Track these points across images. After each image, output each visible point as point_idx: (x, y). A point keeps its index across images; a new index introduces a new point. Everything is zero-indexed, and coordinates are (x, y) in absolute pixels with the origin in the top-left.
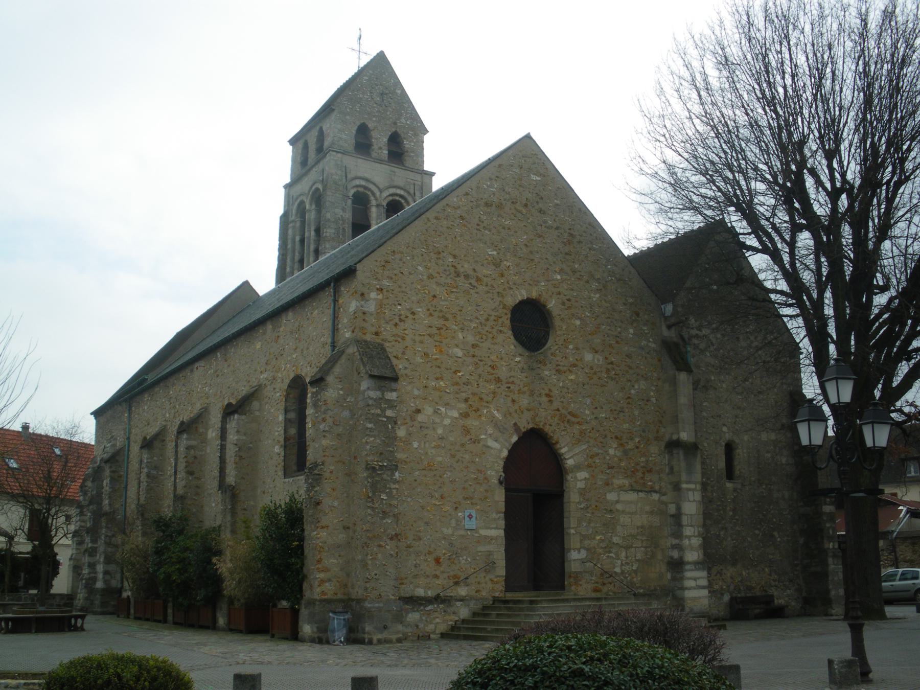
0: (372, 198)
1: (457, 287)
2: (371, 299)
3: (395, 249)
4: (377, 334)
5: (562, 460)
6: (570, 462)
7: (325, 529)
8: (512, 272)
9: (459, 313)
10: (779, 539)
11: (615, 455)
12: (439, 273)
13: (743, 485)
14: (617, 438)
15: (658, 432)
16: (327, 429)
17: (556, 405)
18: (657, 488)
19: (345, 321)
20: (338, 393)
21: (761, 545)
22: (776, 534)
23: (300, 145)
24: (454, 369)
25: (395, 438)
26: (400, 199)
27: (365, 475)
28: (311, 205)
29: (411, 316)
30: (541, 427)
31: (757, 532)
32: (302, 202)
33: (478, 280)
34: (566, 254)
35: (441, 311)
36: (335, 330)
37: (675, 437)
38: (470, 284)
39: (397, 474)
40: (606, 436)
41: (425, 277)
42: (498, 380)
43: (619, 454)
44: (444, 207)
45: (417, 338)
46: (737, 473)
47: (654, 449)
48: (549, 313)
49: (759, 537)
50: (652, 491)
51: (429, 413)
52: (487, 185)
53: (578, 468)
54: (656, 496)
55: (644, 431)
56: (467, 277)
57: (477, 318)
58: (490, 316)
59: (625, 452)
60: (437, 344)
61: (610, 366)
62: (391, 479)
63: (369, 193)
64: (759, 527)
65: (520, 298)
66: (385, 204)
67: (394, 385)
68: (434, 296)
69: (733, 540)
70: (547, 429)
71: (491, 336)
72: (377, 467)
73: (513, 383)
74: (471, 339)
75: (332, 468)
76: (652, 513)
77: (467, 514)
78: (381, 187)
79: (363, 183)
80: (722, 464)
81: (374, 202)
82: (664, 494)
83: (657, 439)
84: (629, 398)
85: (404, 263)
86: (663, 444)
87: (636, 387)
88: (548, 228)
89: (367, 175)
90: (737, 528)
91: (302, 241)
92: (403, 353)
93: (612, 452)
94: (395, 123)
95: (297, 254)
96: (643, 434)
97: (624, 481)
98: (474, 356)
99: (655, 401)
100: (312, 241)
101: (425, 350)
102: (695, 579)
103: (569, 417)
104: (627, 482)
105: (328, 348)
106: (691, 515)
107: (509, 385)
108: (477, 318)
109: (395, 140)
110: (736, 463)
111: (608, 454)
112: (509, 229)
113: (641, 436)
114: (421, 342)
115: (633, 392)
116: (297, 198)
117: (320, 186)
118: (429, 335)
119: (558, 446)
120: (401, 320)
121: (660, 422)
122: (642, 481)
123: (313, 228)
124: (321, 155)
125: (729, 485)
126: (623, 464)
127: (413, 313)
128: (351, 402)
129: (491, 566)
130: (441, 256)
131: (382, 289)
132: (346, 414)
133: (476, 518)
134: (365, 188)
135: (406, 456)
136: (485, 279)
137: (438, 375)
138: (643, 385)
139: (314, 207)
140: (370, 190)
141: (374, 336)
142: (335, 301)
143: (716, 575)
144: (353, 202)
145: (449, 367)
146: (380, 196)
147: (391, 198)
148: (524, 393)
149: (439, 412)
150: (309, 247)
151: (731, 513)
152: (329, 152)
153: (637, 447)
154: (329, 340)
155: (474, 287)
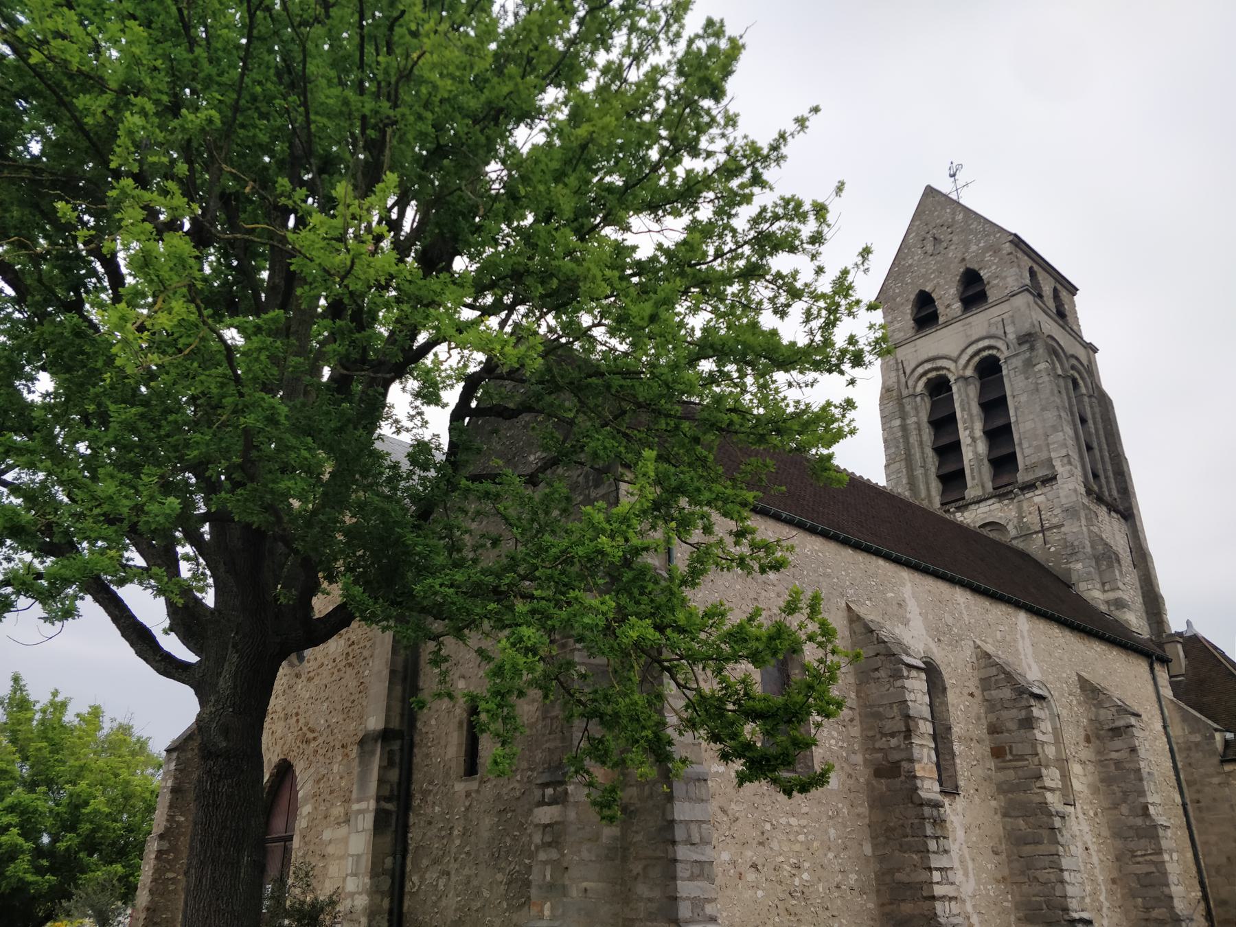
26: (991, 352)
31: (499, 877)
53: (306, 801)
66: (969, 372)
69: (458, 896)
79: (928, 366)
89: (932, 354)
94: (964, 259)
125: (460, 787)
146: (957, 367)
147: (977, 359)
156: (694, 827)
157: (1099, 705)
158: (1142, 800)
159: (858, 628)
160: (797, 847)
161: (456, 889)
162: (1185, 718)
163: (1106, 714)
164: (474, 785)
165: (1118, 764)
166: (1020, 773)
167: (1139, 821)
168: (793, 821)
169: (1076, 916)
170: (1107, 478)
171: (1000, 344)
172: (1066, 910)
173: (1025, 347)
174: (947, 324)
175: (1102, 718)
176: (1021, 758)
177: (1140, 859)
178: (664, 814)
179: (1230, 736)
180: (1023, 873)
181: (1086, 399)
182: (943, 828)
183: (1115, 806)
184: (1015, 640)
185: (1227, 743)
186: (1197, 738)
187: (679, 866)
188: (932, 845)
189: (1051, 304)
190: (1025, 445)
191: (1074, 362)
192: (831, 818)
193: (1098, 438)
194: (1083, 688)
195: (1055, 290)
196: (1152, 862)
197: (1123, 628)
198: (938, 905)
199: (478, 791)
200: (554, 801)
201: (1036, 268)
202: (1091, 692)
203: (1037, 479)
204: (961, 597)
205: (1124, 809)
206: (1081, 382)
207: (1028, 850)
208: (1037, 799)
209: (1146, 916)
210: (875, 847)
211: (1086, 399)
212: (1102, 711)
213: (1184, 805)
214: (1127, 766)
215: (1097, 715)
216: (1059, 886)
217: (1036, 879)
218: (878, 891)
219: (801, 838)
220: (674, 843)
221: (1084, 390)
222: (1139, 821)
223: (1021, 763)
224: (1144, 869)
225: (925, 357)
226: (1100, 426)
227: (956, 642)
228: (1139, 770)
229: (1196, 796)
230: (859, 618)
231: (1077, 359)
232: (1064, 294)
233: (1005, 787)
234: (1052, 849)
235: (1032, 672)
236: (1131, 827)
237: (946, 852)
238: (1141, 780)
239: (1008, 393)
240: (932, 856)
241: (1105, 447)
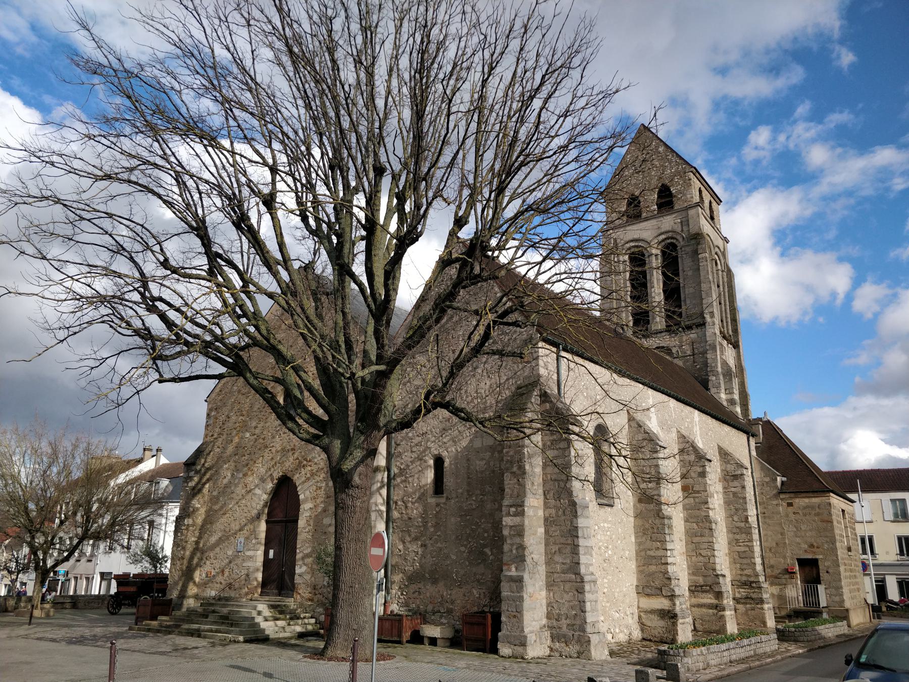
6: (302, 497)
10: (491, 557)
13: (447, 498)
21: (467, 563)
22: (487, 551)
31: (463, 549)
49: (465, 554)
53: (306, 500)
64: (465, 543)
69: (432, 558)
79: (633, 244)
89: (636, 237)
90: (439, 545)
125: (432, 501)
140: (641, 246)
143: (414, 593)
151: (432, 530)
156: (585, 529)
157: (728, 462)
158: (745, 513)
159: (634, 424)
160: (607, 538)
161: (431, 554)
162: (763, 468)
163: (730, 468)
164: (443, 500)
165: (734, 494)
166: (697, 500)
167: (742, 525)
168: (606, 525)
169: (719, 573)
170: (727, 322)
171: (678, 237)
172: (714, 570)
173: (693, 242)
174: (647, 219)
175: (728, 469)
176: (698, 492)
177: (741, 544)
178: (572, 523)
179: (784, 479)
180: (693, 550)
181: (720, 273)
182: (672, 529)
183: (731, 516)
184: (693, 427)
185: (783, 483)
186: (767, 479)
187: (581, 549)
188: (668, 538)
189: (708, 211)
190: (688, 302)
191: (717, 250)
192: (619, 523)
193: (725, 297)
194: (720, 453)
195: (710, 202)
196: (747, 546)
197: (734, 415)
198: (669, 567)
199: (445, 504)
200: (515, 515)
201: (703, 189)
202: (724, 454)
203: (694, 324)
204: (673, 403)
205: (736, 518)
206: (718, 262)
207: (696, 540)
208: (704, 514)
209: (741, 573)
210: (636, 537)
211: (720, 273)
212: (729, 466)
213: (757, 515)
214: (740, 495)
215: (726, 467)
216: (712, 558)
217: (700, 554)
218: (637, 560)
219: (608, 533)
220: (578, 537)
221: (719, 267)
222: (742, 525)
223: (697, 495)
224: (743, 549)
225: (630, 238)
226: (726, 290)
227: (669, 430)
228: (745, 498)
229: (763, 511)
230: (634, 419)
231: (719, 248)
232: (714, 204)
233: (688, 507)
234: (710, 540)
235: (653, 424)
236: (738, 527)
237: (673, 541)
238: (746, 503)
239: (680, 268)
240: (668, 543)
241: (728, 303)
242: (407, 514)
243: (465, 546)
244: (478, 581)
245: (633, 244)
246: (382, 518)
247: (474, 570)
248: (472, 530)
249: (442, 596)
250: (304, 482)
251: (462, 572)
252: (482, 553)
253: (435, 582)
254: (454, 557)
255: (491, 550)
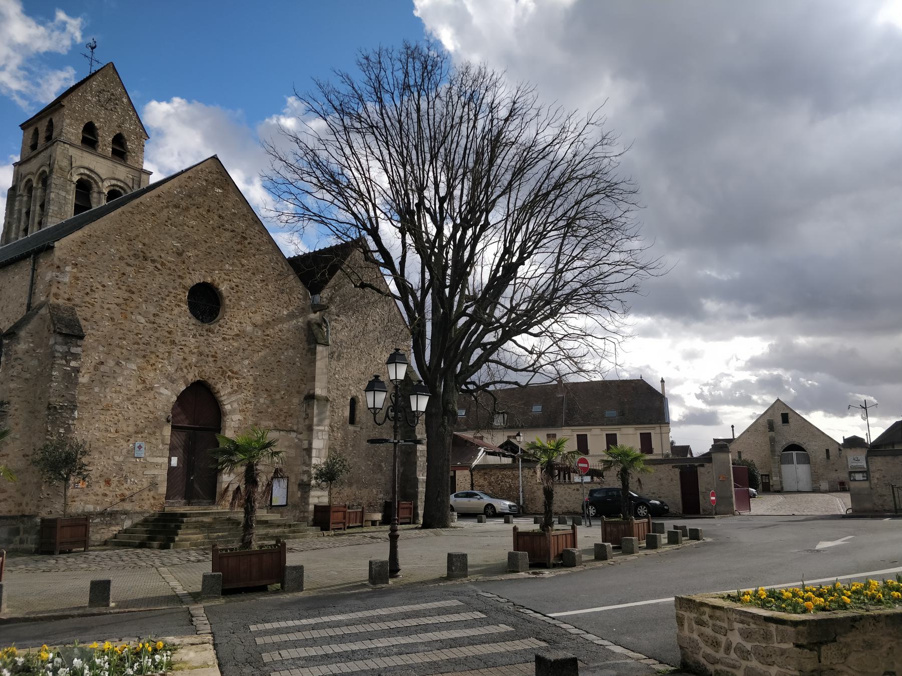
0: (94, 186)
1: (144, 269)
2: (66, 272)
3: (92, 234)
4: (69, 299)
5: (221, 405)
6: (228, 407)
7: (5, 457)
8: (191, 261)
9: (144, 289)
11: (264, 403)
12: (129, 256)
13: (361, 428)
14: (266, 390)
15: (299, 387)
16: (15, 374)
17: (219, 364)
18: (295, 428)
19: (42, 287)
20: (29, 346)
22: (383, 464)
23: (31, 131)
24: (136, 331)
25: (77, 384)
26: (120, 190)
27: (46, 413)
28: (38, 184)
29: (101, 288)
30: (206, 380)
31: (369, 463)
32: (30, 180)
33: (163, 264)
34: (238, 251)
35: (129, 286)
36: (32, 293)
37: (311, 392)
38: (156, 267)
39: (76, 413)
40: (258, 389)
41: (117, 258)
42: (173, 342)
43: (267, 402)
44: (138, 204)
45: (106, 306)
46: (357, 419)
47: (296, 401)
48: (220, 293)
50: (291, 430)
51: (111, 366)
52: (177, 191)
53: (233, 411)
54: (293, 435)
55: (289, 386)
56: (153, 261)
57: (159, 293)
58: (171, 293)
59: (273, 401)
60: (123, 311)
61: (265, 338)
62: (71, 416)
63: (92, 181)
65: (198, 281)
67: (79, 342)
68: (124, 274)
70: (210, 381)
71: (170, 308)
72: (58, 407)
73: (185, 345)
74: (152, 310)
75: (17, 406)
76: (289, 447)
77: (137, 445)
78: (104, 177)
80: (347, 413)
81: (95, 189)
82: (301, 433)
83: (298, 392)
84: (279, 361)
85: (99, 245)
86: (302, 397)
87: (286, 354)
88: (225, 230)
89: (92, 167)
90: (355, 460)
91: (28, 213)
92: (92, 317)
93: (262, 401)
95: (22, 224)
96: (288, 388)
97: (270, 423)
98: (154, 323)
99: (299, 365)
100: (37, 215)
101: (112, 315)
102: (318, 497)
103: (230, 373)
104: (271, 424)
105: (25, 307)
106: (319, 449)
107: (182, 347)
108: (159, 293)
109: (119, 140)
110: (357, 412)
111: (259, 402)
112: (192, 227)
113: (286, 390)
114: (109, 309)
115: (282, 357)
116: (25, 177)
117: (47, 170)
118: (116, 304)
119: (219, 395)
120: (92, 290)
121: (302, 380)
122: (284, 423)
123: (38, 204)
124: (49, 143)
125: (351, 428)
126: (270, 410)
127: (104, 286)
128: (41, 353)
129: (153, 485)
130: (132, 243)
131: (77, 265)
132: (35, 362)
133: (145, 448)
134: (88, 176)
135: (87, 398)
136: (169, 265)
137: (122, 336)
138: (291, 352)
139: (40, 185)
140: (93, 178)
141: (66, 302)
142: (34, 270)
144: (77, 187)
145: (131, 330)
148: (193, 353)
149: (120, 365)
150: (33, 219)
151: (351, 449)
152: (56, 141)
153: (282, 398)
154: (26, 302)
155: (159, 269)
199: (360, 432)
242: (334, 436)
243: (371, 461)
244: (377, 483)
245: (88, 173)
246: (521, 449)
247: (375, 476)
248: (375, 450)
249: (355, 495)
250: (230, 394)
251: (368, 478)
252: (380, 466)
253: (350, 485)
254: (363, 468)
255: (385, 464)
